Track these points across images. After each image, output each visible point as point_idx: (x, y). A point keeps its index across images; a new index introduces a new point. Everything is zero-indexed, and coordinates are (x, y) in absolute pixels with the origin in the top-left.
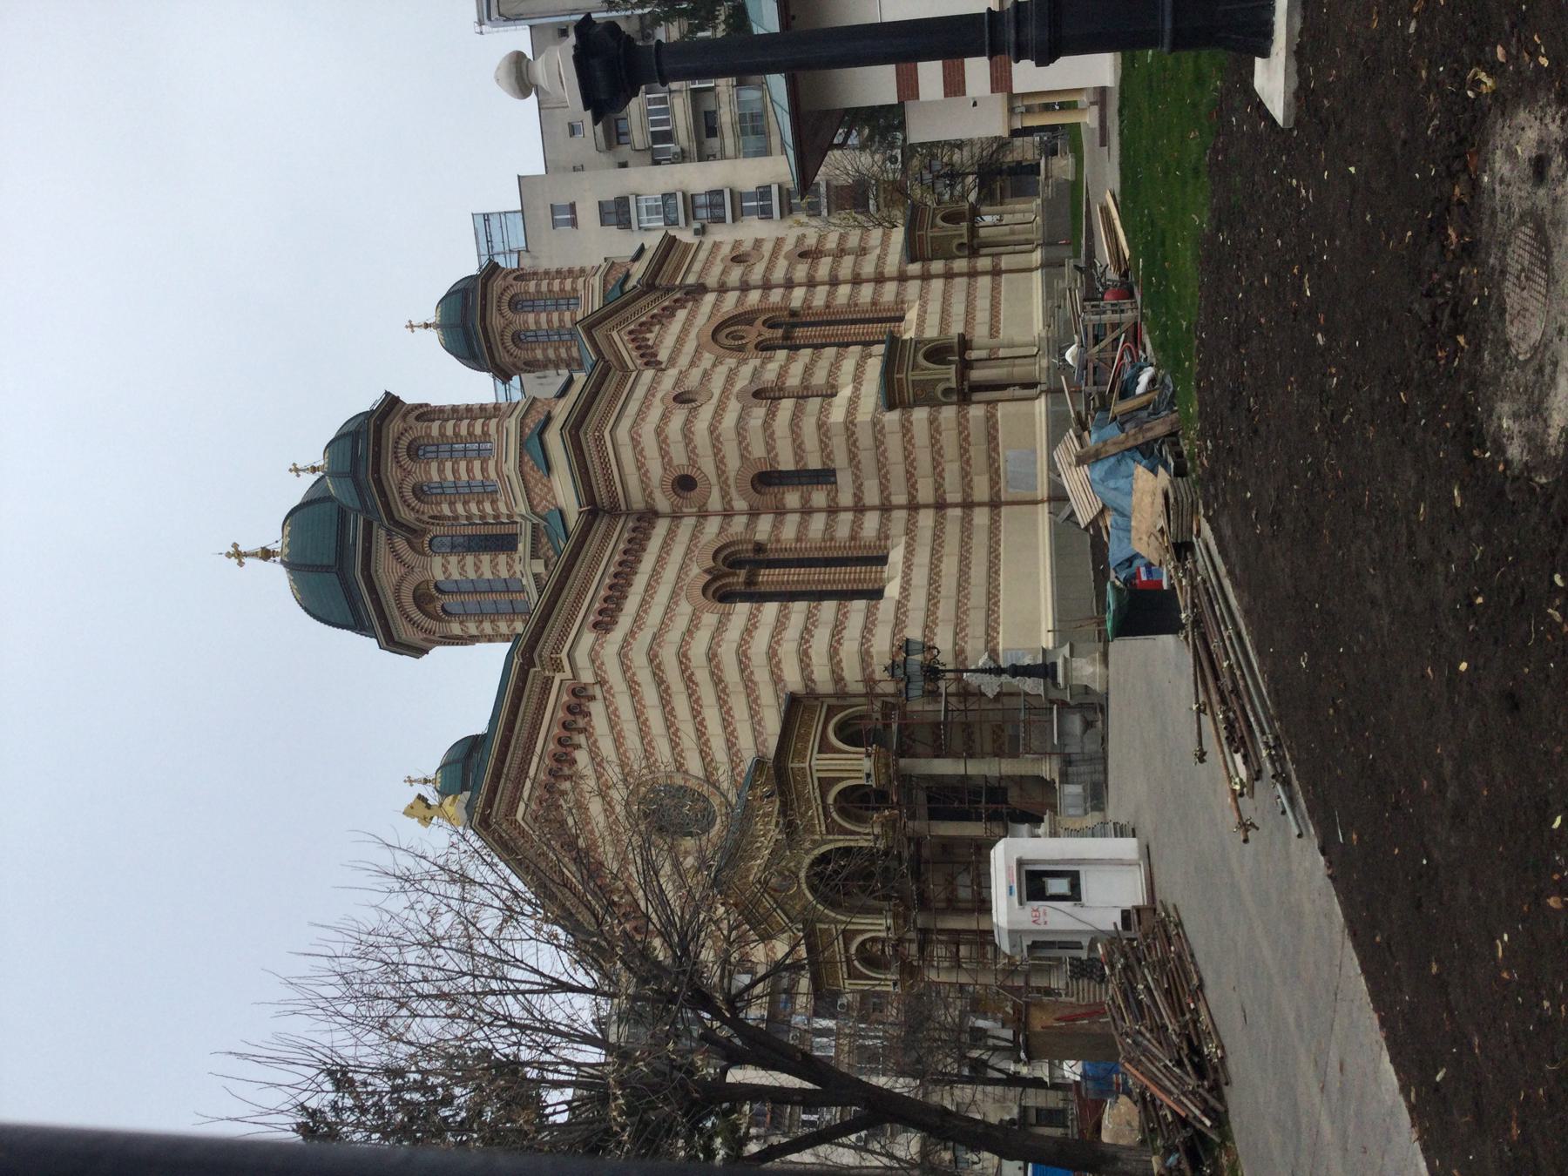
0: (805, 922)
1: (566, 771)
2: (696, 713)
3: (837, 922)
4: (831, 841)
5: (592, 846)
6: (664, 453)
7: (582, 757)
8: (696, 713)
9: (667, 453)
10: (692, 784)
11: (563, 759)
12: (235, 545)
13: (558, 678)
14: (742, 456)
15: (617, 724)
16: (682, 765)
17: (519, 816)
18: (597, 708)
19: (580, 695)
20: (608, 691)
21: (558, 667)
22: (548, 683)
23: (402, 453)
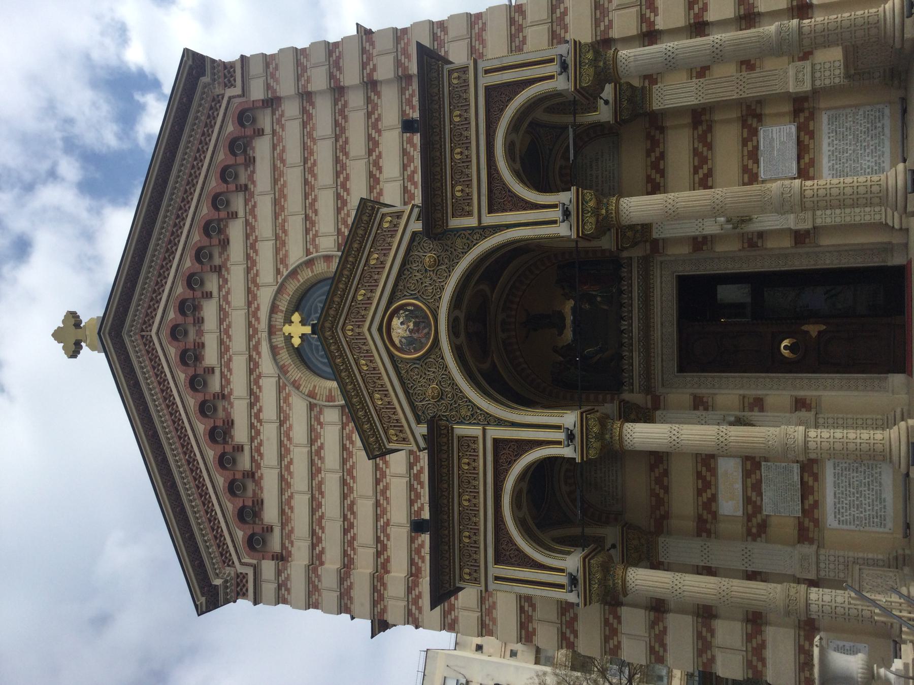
1: (217, 261)
2: (372, 145)
5: (223, 396)
7: (235, 231)
8: (372, 145)
11: (214, 230)
13: (229, 92)
17: (153, 333)
18: (262, 148)
19: (245, 117)
20: (279, 121)
21: (230, 84)
22: (217, 99)
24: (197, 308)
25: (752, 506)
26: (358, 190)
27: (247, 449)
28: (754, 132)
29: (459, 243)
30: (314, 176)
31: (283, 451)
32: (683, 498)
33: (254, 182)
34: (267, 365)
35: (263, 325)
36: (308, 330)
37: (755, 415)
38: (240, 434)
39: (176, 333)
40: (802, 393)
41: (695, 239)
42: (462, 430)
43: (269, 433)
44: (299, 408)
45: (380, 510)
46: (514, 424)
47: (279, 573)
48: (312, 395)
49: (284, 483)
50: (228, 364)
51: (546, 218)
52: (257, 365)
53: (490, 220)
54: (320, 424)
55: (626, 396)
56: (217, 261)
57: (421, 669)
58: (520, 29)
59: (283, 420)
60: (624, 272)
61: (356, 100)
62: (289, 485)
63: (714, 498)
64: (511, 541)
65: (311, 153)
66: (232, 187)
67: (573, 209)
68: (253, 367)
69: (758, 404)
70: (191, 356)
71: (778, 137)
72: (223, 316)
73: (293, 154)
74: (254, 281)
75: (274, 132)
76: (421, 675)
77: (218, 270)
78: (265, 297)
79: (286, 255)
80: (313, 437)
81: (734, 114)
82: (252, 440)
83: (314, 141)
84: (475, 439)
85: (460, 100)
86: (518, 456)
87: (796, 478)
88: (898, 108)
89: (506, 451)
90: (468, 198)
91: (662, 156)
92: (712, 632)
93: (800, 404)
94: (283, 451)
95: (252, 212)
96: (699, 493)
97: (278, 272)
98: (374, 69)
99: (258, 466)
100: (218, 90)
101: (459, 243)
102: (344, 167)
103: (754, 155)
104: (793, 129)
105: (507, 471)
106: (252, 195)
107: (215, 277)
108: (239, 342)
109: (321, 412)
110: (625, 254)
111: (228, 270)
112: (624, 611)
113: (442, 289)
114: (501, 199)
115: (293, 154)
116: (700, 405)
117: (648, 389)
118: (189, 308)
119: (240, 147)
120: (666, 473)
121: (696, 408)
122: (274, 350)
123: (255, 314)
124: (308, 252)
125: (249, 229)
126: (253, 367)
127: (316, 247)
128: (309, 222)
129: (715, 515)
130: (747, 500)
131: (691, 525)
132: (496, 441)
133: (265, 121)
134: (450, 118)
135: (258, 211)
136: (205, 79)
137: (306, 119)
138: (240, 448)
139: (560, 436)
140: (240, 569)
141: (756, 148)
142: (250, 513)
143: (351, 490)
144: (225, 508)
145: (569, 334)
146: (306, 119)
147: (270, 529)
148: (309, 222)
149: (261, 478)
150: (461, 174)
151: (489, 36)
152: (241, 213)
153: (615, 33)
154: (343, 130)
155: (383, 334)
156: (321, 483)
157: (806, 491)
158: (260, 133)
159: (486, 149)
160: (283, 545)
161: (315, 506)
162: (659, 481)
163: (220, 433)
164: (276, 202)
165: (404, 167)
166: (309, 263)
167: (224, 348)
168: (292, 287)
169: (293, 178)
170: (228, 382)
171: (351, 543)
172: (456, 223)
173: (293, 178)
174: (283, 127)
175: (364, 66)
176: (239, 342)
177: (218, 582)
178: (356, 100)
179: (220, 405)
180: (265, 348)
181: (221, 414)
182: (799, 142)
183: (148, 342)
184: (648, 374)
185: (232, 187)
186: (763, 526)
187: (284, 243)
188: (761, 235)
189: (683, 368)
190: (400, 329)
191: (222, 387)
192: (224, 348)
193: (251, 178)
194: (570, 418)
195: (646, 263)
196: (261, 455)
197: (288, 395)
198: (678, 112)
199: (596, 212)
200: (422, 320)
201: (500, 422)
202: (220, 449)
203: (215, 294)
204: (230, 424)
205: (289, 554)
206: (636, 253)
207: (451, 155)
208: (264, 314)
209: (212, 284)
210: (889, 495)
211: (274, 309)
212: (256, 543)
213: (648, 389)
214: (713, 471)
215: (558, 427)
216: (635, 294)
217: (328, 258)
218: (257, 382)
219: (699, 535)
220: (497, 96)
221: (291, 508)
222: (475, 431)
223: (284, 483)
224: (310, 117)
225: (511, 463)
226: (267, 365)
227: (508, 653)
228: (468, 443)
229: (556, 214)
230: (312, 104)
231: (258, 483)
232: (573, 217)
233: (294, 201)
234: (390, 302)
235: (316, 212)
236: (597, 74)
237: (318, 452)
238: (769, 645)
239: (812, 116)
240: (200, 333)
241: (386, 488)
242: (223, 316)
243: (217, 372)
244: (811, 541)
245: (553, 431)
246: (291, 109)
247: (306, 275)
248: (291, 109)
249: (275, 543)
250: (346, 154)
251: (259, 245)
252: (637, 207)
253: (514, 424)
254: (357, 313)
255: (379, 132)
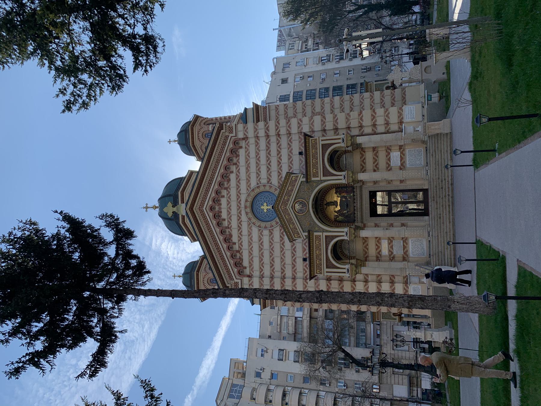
0: (309, 232)
1: (226, 186)
2: (279, 152)
3: (324, 231)
4: (325, 181)
6: (286, 113)
7: (233, 177)
8: (279, 152)
9: (287, 112)
10: (272, 190)
11: (225, 177)
12: (147, 204)
13: (231, 135)
14: (312, 112)
15: (248, 160)
16: (270, 180)
17: (204, 209)
18: (242, 152)
19: (236, 143)
22: (227, 137)
23: (202, 123)
24: (219, 201)
25: (391, 252)
26: (285, 170)
27: (237, 244)
28: (389, 154)
29: (315, 184)
30: (260, 161)
31: (250, 244)
32: (372, 251)
33: (239, 163)
34: (244, 218)
35: (243, 206)
36: (270, 207)
37: (391, 228)
38: (235, 239)
39: (212, 209)
40: (403, 222)
41: (374, 181)
42: (315, 234)
43: (245, 239)
44: (255, 230)
45: (282, 260)
46: (330, 232)
47: (250, 281)
48: (259, 226)
49: (250, 254)
50: (230, 218)
51: (340, 178)
52: (240, 218)
53: (323, 178)
54: (262, 235)
55: (356, 224)
56: (226, 186)
57: (247, 346)
58: (324, 123)
59: (250, 234)
60: (355, 190)
61: (273, 139)
62: (252, 254)
63: (380, 251)
64: (331, 262)
65: (258, 154)
66: (232, 164)
67: (346, 176)
68: (239, 218)
69: (392, 225)
70: (217, 216)
71: (395, 155)
72: (229, 203)
73: (253, 154)
74: (239, 192)
75: (246, 148)
76: (247, 349)
77: (226, 189)
78: (243, 198)
79: (250, 184)
80: (260, 239)
81: (384, 149)
82: (239, 241)
83: (259, 151)
84: (320, 236)
85: (315, 146)
86: (332, 240)
87: (402, 244)
88: (425, 149)
89: (329, 239)
90: (317, 172)
91: (365, 159)
92: (381, 286)
93: (403, 225)
94: (250, 244)
95: (238, 171)
96: (377, 249)
97: (247, 189)
98: (280, 131)
99: (241, 249)
100: (227, 134)
101: (315, 184)
102: (269, 159)
103: (389, 159)
104: (399, 153)
105: (329, 244)
106: (238, 166)
107: (226, 191)
108: (234, 211)
109: (262, 231)
110: (355, 185)
111: (230, 189)
112: (357, 283)
113: (310, 196)
114: (326, 173)
115: (253, 154)
116: (376, 225)
117: (362, 222)
118: (216, 201)
119: (234, 152)
120: (367, 245)
121: (375, 227)
122: (247, 213)
123: (239, 202)
124: (258, 184)
125: (238, 176)
126: (239, 218)
127: (260, 182)
128: (258, 174)
129: (381, 255)
130: (390, 251)
131: (375, 258)
132: (326, 236)
133: (243, 144)
134: (311, 152)
135: (241, 171)
136: (224, 131)
137: (257, 144)
138: (235, 243)
139: (344, 234)
140: (236, 280)
141: (390, 158)
142: (238, 264)
143: (273, 255)
144: (230, 263)
145: (339, 208)
146: (257, 144)
147: (245, 268)
148: (258, 174)
149: (242, 252)
150: (315, 166)
151: (315, 124)
152: (235, 172)
153: (351, 126)
154: (269, 148)
155: (292, 207)
156: (262, 253)
157: (404, 247)
158: (241, 147)
159: (321, 160)
160: (250, 273)
161: (261, 260)
162: (365, 247)
163: (228, 240)
164: (247, 168)
165: (300, 164)
166: (258, 187)
167: (229, 213)
168: (253, 194)
169: (253, 162)
170: (230, 223)
171: (273, 270)
172: (313, 179)
173: (253, 162)
174: (249, 146)
175: (276, 130)
176: (234, 211)
177: (228, 285)
178: (273, 139)
179: (227, 230)
180: (243, 212)
181: (227, 233)
182: (401, 156)
183: (202, 211)
184: (362, 218)
185: (232, 164)
186: (394, 257)
187: (249, 181)
188: (391, 181)
189: (371, 216)
190: (297, 207)
191: (228, 225)
192: (229, 213)
193: (238, 161)
194: (346, 230)
195: (361, 187)
196: (242, 246)
197: (251, 227)
198: (369, 148)
199: (352, 177)
200: (304, 205)
201: (327, 231)
202: (228, 244)
203: (226, 196)
204: (231, 236)
205: (252, 275)
206: (359, 185)
207: (312, 161)
208: (243, 202)
209: (224, 192)
210: (425, 248)
211: (246, 201)
212: (240, 273)
213: (362, 222)
214: (380, 243)
215: (343, 232)
216: (358, 196)
217: (264, 186)
218: (240, 223)
219: (377, 261)
220: (325, 147)
221: (253, 261)
222: (320, 234)
223: (250, 254)
224: (258, 143)
225: (330, 242)
226: (244, 218)
227: (282, 338)
228: (318, 237)
229: (342, 177)
230: (259, 140)
231: (241, 254)
232: (346, 178)
233: (253, 168)
234: (295, 200)
235: (260, 172)
236: (352, 143)
237: (261, 244)
238: (396, 288)
239: (404, 150)
240: (220, 208)
241: (284, 253)
242: (229, 203)
243: (226, 220)
244: (406, 260)
245: (342, 233)
246: (252, 141)
247: (257, 191)
248: (252, 141)
249: (247, 271)
250: (270, 155)
251: (240, 181)
252: (362, 176)
253: (330, 232)
254: (285, 203)
255: (281, 149)
